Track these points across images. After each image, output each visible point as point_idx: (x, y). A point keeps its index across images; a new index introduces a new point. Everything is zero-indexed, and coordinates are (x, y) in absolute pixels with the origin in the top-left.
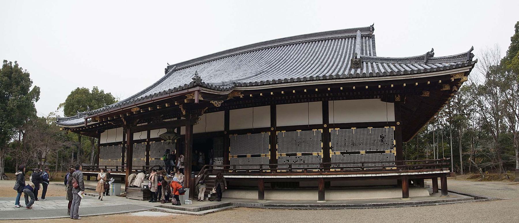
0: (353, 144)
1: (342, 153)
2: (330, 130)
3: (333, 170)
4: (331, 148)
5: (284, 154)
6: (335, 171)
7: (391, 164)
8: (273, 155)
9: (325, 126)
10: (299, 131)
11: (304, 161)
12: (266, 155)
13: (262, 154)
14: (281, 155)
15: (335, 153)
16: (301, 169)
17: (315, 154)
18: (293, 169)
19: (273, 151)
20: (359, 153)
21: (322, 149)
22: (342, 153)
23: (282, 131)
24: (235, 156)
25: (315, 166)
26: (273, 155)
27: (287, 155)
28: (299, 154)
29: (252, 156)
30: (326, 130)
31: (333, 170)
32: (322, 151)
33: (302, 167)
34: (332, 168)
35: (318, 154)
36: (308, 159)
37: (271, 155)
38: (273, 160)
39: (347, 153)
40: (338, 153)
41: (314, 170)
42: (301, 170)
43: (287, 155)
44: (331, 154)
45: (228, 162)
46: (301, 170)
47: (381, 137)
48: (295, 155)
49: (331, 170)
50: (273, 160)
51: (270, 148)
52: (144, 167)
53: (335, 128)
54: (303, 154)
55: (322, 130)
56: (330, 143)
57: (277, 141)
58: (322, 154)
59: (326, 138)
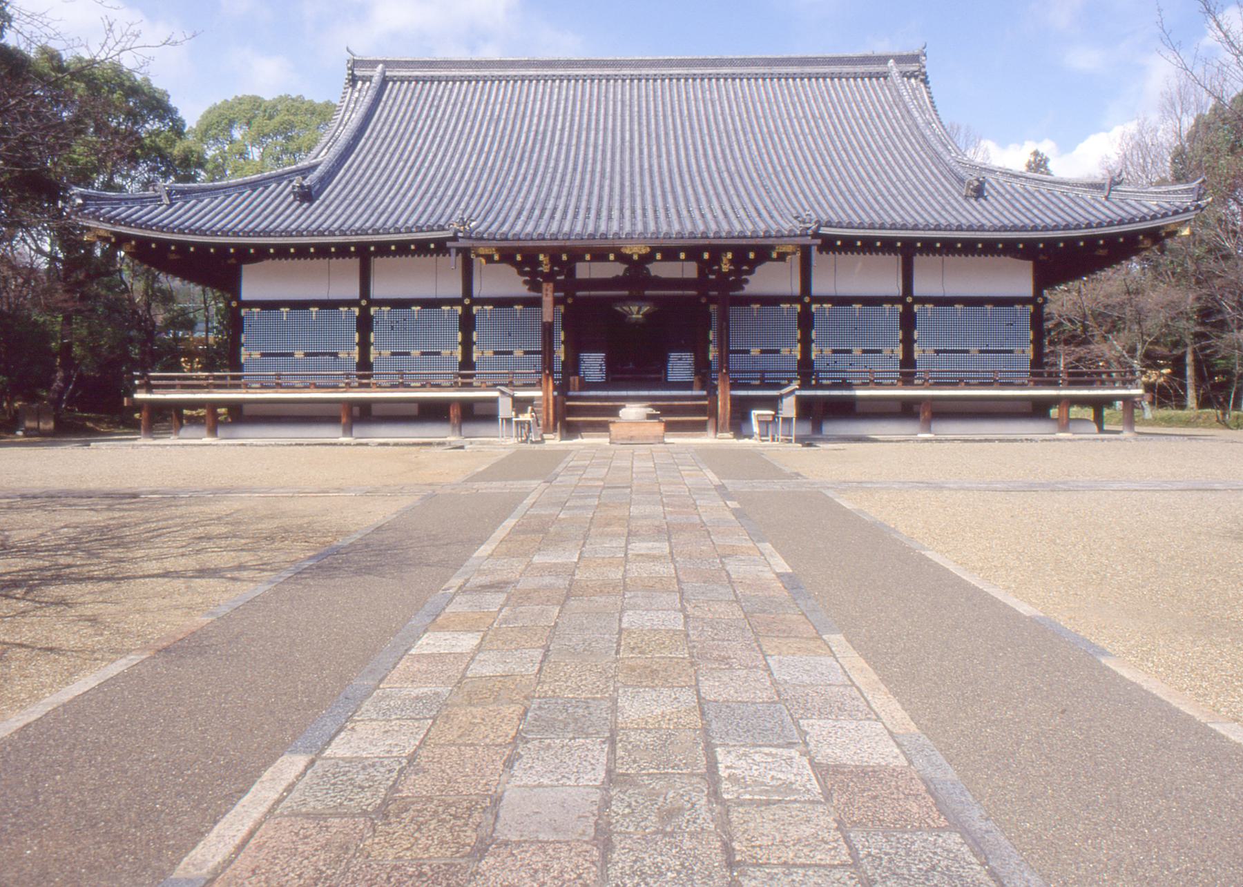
3: (920, 382)
5: (827, 351)
9: (807, 300)
15: (924, 351)
16: (785, 379)
18: (822, 379)
19: (806, 343)
23: (825, 305)
30: (908, 309)
31: (920, 382)
33: (863, 375)
34: (919, 378)
35: (892, 351)
51: (799, 336)
55: (798, 307)
59: (908, 322)
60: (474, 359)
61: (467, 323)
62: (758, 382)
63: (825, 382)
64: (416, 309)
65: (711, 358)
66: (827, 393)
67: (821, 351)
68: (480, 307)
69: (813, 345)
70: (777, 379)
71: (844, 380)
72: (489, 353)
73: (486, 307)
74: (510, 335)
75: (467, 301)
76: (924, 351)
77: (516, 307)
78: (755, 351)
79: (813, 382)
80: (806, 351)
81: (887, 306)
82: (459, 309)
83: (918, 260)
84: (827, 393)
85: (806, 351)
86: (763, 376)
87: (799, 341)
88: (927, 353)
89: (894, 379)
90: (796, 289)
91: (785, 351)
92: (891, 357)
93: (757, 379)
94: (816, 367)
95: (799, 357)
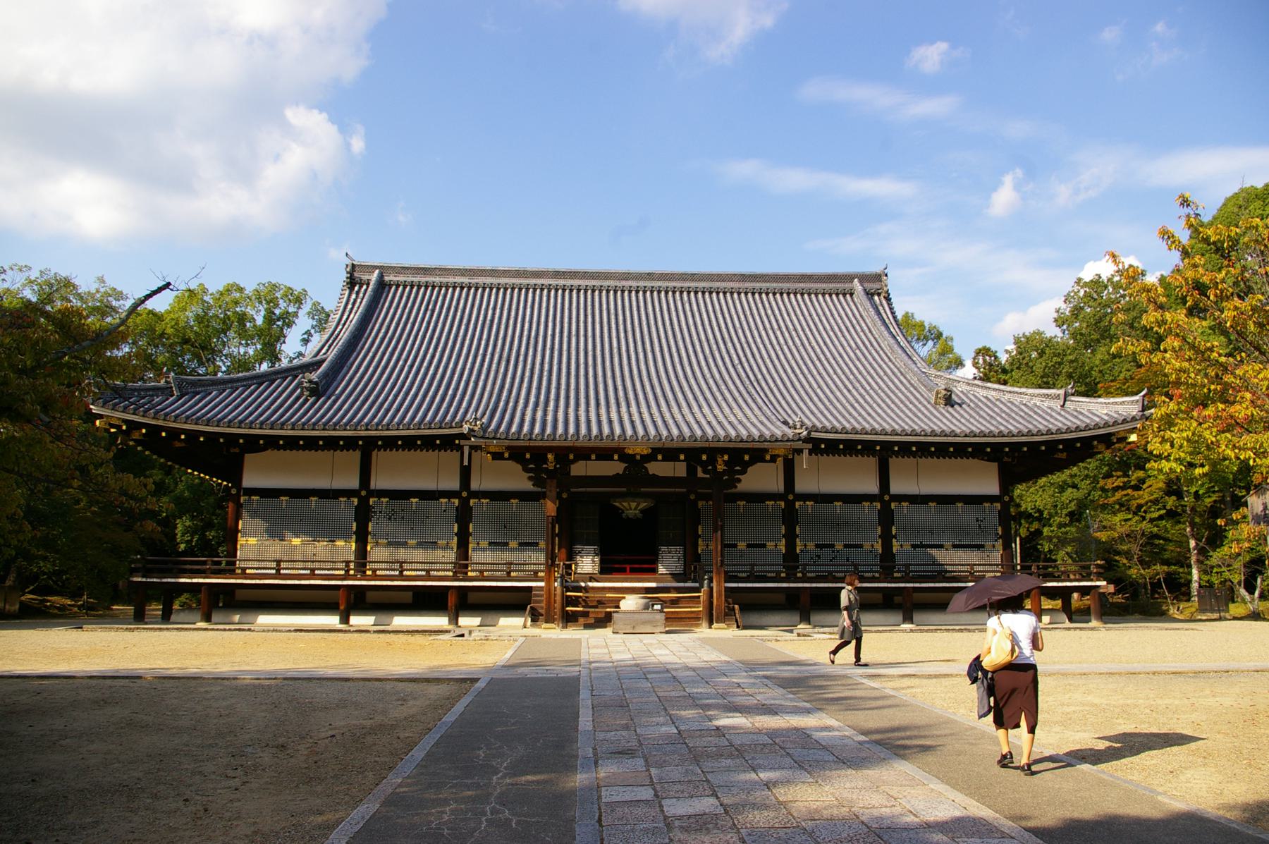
1: (914, 546)
2: (797, 504)
3: (899, 575)
5: (811, 545)
7: (995, 568)
9: (791, 497)
11: (848, 560)
14: (805, 546)
15: (901, 546)
17: (867, 545)
19: (791, 538)
21: (880, 537)
23: (808, 503)
25: (774, 568)
27: (817, 546)
28: (839, 545)
31: (899, 575)
32: (880, 541)
34: (898, 572)
35: (872, 546)
36: (856, 556)
38: (791, 556)
40: (907, 546)
43: (817, 546)
44: (896, 545)
47: (977, 521)
48: (832, 546)
49: (895, 575)
50: (791, 556)
51: (783, 532)
52: (348, 563)
54: (846, 546)
55: (783, 504)
56: (894, 529)
58: (879, 547)
59: (886, 518)
62: (744, 575)
64: (414, 500)
65: (700, 552)
66: (814, 585)
67: (805, 546)
68: (476, 500)
69: (797, 540)
70: (761, 571)
71: (830, 573)
75: (464, 494)
77: (512, 501)
78: (742, 545)
80: (791, 545)
81: (866, 504)
82: (456, 501)
83: (893, 462)
84: (814, 585)
85: (791, 545)
87: (784, 536)
90: (781, 488)
91: (770, 545)
92: (871, 552)
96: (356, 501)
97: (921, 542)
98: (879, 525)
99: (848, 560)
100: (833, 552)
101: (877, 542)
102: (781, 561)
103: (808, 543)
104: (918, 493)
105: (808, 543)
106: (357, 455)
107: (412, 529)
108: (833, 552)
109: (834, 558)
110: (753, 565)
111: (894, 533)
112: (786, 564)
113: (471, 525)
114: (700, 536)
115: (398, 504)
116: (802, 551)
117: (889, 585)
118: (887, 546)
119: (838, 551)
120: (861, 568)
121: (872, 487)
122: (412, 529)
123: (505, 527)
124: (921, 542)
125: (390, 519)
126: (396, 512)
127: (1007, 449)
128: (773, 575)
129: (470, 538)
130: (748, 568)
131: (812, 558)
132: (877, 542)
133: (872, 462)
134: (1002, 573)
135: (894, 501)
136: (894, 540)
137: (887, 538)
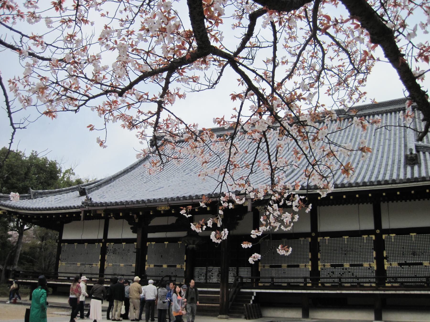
0: (414, 254)
1: (400, 264)
3: (389, 285)
4: (386, 258)
5: (328, 265)
6: (392, 287)
8: (315, 266)
9: (378, 231)
10: (346, 237)
11: (353, 274)
12: (305, 266)
13: (301, 265)
15: (391, 264)
17: (366, 265)
19: (315, 261)
20: (421, 264)
22: (400, 264)
23: (325, 238)
24: (267, 267)
26: (315, 266)
27: (332, 266)
29: (289, 266)
30: (379, 237)
31: (389, 285)
32: (375, 261)
34: (388, 283)
35: (370, 265)
36: (358, 272)
37: (312, 266)
38: (315, 272)
39: (406, 264)
40: (395, 264)
41: (366, 285)
42: (349, 285)
43: (332, 266)
45: (258, 273)
46: (349, 285)
48: (342, 265)
50: (315, 272)
51: (310, 257)
53: (390, 234)
54: (351, 265)
55: (374, 237)
57: (319, 248)
60: (146, 269)
61: (104, 252)
62: (268, 284)
63: (346, 285)
64: (124, 244)
68: (149, 243)
71: (359, 283)
72: (152, 266)
73: (152, 243)
74: (162, 256)
76: (264, 266)
77: (165, 243)
79: (320, 285)
81: (365, 236)
86: (273, 280)
88: (266, 268)
89: (372, 283)
91: (302, 265)
92: (369, 269)
93: (302, 283)
94: (388, 274)
95: (310, 269)
96: (310, 239)
97: (406, 261)
98: (310, 252)
99: (353, 274)
100: (343, 269)
101: (373, 262)
102: (374, 275)
103: (326, 264)
104: (388, 228)
105: (326, 264)
106: (103, 221)
107: (122, 258)
108: (343, 269)
109: (343, 274)
110: (272, 278)
111: (385, 255)
112: (312, 277)
113: (147, 256)
114: (319, 260)
115: (117, 246)
116: (322, 269)
117: (361, 292)
118: (380, 265)
119: (346, 269)
120: (343, 280)
121: (371, 226)
122: (122, 258)
123: (162, 256)
124: (406, 261)
125: (114, 253)
126: (116, 250)
127: (357, 196)
128: (286, 285)
129: (146, 263)
130: (270, 280)
131: (329, 274)
132: (373, 262)
133: (369, 207)
134: (376, 284)
135: (385, 234)
136: (385, 260)
137: (380, 260)
